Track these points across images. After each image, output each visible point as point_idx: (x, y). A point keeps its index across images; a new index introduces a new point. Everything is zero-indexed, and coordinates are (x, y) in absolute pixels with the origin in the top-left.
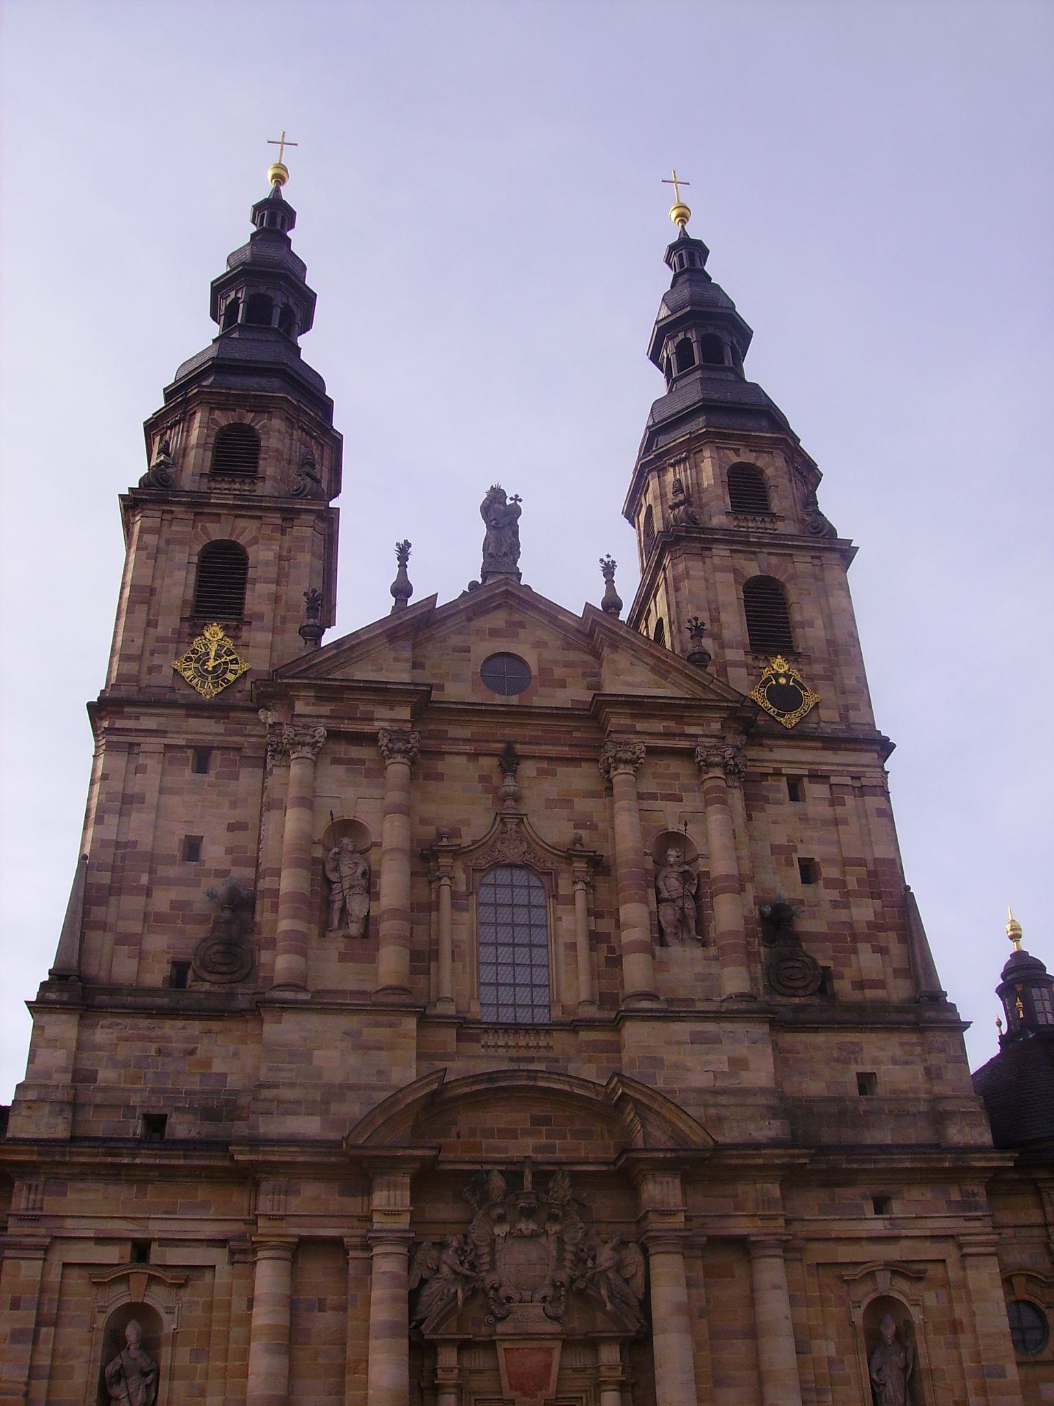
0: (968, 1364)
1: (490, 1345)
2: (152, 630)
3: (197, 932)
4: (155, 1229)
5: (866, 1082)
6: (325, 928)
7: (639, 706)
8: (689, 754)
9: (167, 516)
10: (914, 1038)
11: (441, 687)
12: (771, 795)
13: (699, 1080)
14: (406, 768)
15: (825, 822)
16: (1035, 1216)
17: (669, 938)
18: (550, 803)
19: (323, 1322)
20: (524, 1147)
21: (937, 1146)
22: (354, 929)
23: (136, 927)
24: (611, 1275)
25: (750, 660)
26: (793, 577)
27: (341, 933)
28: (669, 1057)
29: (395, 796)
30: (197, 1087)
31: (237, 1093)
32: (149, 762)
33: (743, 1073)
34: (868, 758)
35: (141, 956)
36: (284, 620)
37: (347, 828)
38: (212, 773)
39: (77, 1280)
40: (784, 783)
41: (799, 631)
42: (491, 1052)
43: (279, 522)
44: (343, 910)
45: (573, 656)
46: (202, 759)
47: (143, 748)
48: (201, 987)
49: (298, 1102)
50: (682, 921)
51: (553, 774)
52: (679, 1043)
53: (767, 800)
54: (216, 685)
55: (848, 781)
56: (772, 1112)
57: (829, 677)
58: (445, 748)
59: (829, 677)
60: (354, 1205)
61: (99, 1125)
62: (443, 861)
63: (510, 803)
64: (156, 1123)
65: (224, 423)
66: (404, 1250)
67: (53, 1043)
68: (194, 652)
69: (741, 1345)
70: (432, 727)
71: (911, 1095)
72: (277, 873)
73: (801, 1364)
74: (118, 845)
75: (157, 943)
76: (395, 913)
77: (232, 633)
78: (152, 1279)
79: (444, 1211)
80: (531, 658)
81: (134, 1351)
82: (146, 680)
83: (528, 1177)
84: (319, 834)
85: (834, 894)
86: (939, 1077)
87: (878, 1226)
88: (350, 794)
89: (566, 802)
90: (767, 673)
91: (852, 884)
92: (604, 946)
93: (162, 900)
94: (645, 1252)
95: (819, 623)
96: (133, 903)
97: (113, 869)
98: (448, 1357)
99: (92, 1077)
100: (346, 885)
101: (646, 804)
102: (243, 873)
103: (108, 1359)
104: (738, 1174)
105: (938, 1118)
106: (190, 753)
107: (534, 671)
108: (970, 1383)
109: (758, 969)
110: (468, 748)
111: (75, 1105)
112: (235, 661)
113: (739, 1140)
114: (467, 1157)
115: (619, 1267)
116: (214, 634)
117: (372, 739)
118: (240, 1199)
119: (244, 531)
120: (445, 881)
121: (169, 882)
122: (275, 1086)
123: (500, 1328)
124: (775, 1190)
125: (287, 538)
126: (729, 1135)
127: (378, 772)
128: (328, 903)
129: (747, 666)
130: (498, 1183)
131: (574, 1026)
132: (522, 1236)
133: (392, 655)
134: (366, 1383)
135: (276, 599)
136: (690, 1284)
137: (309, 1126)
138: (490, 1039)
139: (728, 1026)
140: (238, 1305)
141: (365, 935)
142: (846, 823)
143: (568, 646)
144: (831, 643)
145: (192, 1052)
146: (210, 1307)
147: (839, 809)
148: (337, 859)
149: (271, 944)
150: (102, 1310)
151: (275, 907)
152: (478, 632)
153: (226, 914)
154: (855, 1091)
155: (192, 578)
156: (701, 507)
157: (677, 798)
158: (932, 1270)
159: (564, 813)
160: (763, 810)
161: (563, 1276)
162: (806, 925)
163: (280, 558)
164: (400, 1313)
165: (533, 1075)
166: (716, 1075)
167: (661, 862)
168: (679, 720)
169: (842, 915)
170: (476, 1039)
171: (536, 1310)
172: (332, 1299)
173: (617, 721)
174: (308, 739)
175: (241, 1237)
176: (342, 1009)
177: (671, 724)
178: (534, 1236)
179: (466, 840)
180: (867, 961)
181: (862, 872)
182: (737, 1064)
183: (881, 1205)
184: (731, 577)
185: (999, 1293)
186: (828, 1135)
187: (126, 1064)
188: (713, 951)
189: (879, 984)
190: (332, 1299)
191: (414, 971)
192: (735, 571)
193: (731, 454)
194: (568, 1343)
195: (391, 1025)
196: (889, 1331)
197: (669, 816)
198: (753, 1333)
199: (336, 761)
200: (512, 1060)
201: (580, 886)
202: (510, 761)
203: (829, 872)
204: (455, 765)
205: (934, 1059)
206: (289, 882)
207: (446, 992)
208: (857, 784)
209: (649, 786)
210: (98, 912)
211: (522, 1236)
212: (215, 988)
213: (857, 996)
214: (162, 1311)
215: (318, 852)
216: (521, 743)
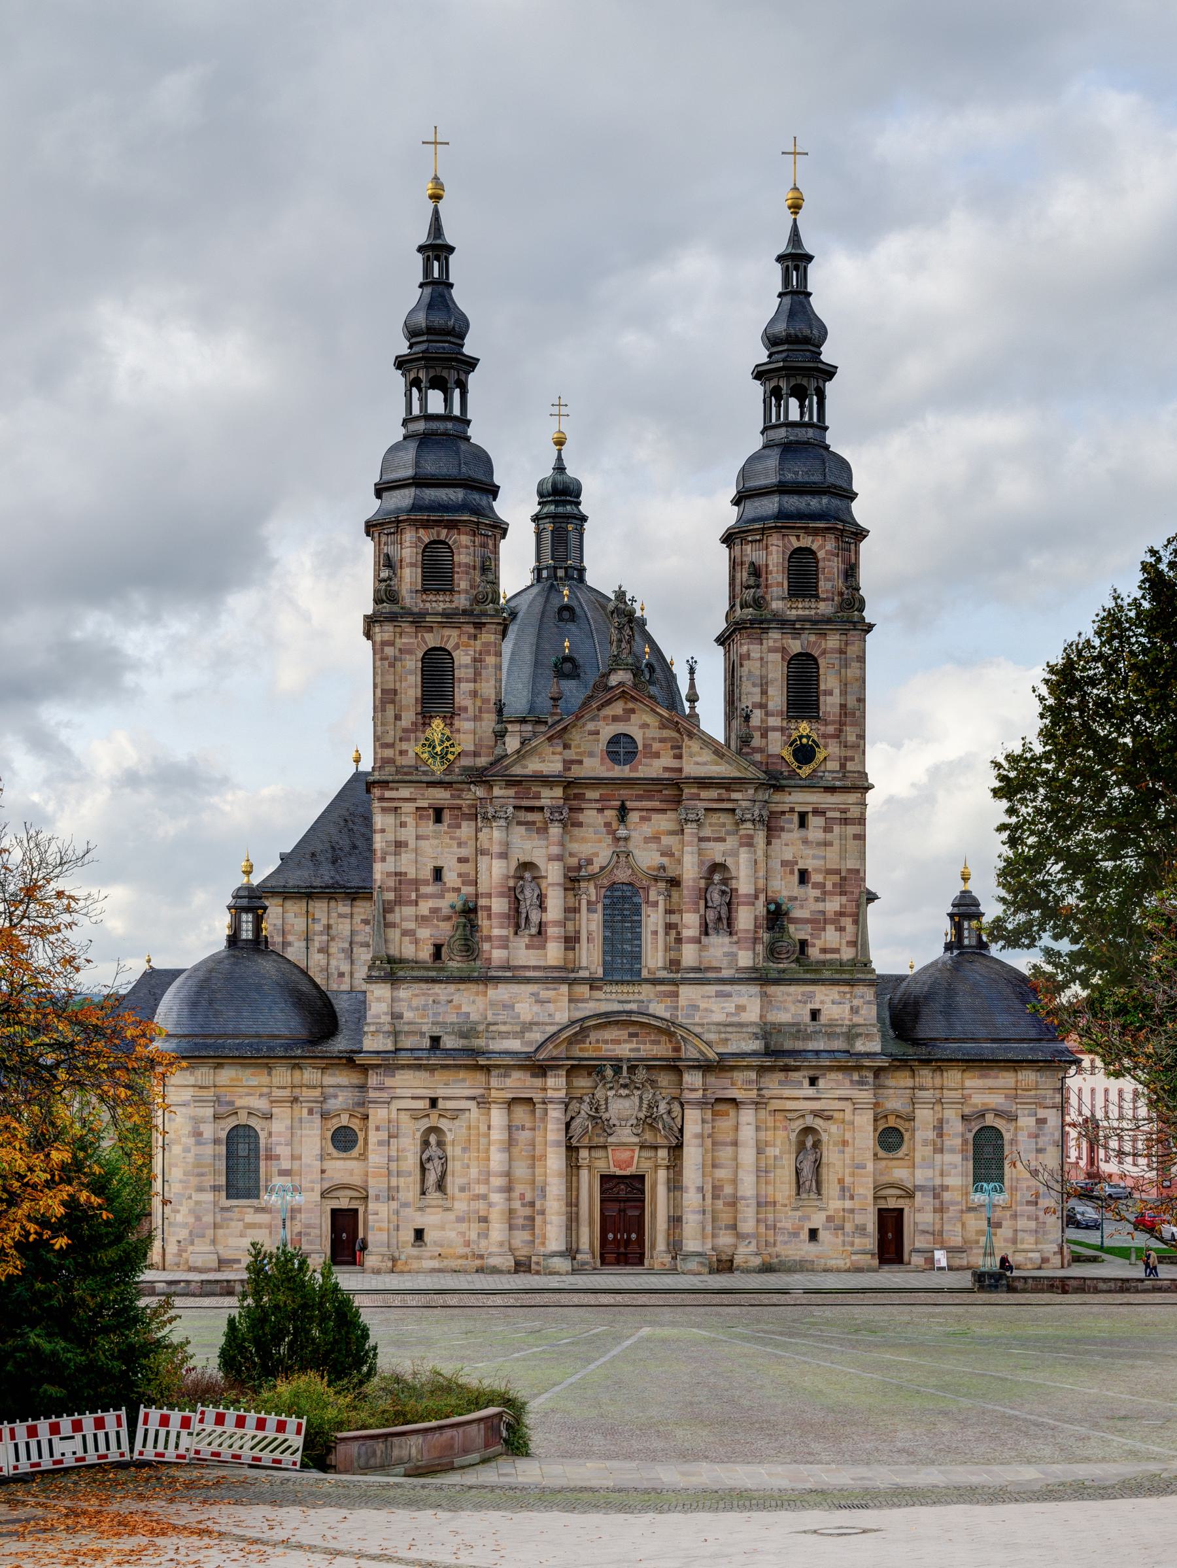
0: (848, 1162)
1: (605, 1147)
2: (398, 723)
3: (444, 931)
4: (440, 1093)
5: (815, 1014)
6: (517, 926)
7: (704, 783)
8: (733, 810)
9: (398, 630)
10: (847, 989)
11: (580, 762)
12: (786, 826)
13: (719, 1017)
14: (561, 830)
15: (819, 844)
16: (909, 1083)
17: (710, 931)
18: (647, 840)
19: (523, 1136)
20: (625, 1050)
21: (848, 1052)
22: (534, 931)
23: (411, 925)
24: (665, 1116)
25: (785, 724)
26: (824, 652)
27: (527, 932)
28: (703, 1005)
29: (555, 850)
30: (455, 1020)
31: (477, 1023)
32: (408, 819)
34: (852, 798)
35: (416, 942)
36: (480, 711)
37: (527, 866)
38: (446, 824)
39: (405, 1117)
40: (796, 818)
41: (822, 698)
42: (608, 996)
43: (472, 631)
44: (527, 917)
45: (667, 733)
46: (438, 815)
47: (403, 810)
48: (454, 963)
49: (508, 1033)
50: (720, 919)
51: (649, 819)
52: (709, 997)
53: (782, 829)
54: (442, 763)
55: (837, 815)
56: (756, 1036)
57: (837, 735)
58: (583, 806)
59: (838, 737)
60: (538, 1082)
61: (407, 1042)
62: (583, 884)
63: (622, 843)
64: (435, 1040)
65: (427, 540)
66: (563, 1106)
67: (379, 1000)
68: (427, 739)
69: (730, 1149)
70: (576, 791)
71: (840, 1022)
72: (489, 896)
73: (757, 1159)
74: (396, 874)
75: (424, 933)
76: (556, 923)
77: (448, 721)
78: (440, 1115)
79: (583, 1082)
80: (638, 736)
81: (434, 1148)
82: (402, 761)
83: (625, 1068)
84: (512, 873)
85: (817, 893)
86: (857, 1012)
87: (811, 1092)
88: (528, 845)
89: (656, 838)
90: (795, 734)
91: (829, 887)
92: (674, 932)
93: (424, 907)
94: (682, 1105)
95: (837, 692)
96: (409, 911)
97: (395, 890)
98: (584, 1153)
99: (400, 1016)
100: (528, 903)
101: (704, 845)
102: (468, 890)
103: (423, 1152)
104: (733, 1068)
106: (431, 811)
107: (640, 748)
108: (847, 1171)
109: (760, 948)
110: (598, 805)
111: (396, 1034)
112: (452, 745)
113: (737, 1051)
114: (594, 1055)
115: (669, 1112)
116: (437, 724)
117: (541, 809)
118: (480, 1077)
119: (450, 638)
120: (584, 896)
121: (427, 896)
122: (495, 1024)
123: (610, 1140)
124: (753, 1075)
125: (478, 642)
126: (732, 1048)
127: (543, 830)
128: (517, 911)
129: (782, 729)
130: (609, 1073)
131: (655, 982)
132: (621, 1096)
133: (551, 749)
134: (545, 1166)
135: (475, 694)
136: (703, 1121)
137: (515, 1045)
138: (607, 988)
139: (737, 988)
140: (483, 1128)
141: (540, 933)
142: (831, 844)
143: (663, 727)
144: (843, 706)
145: (451, 1001)
146: (469, 1128)
147: (829, 836)
148: (522, 887)
149: (489, 938)
150: (418, 1130)
151: (489, 917)
152: (605, 718)
153: (463, 920)
154: (807, 1018)
155: (419, 679)
156: (767, 586)
158: (836, 1115)
159: (654, 846)
160: (779, 837)
161: (642, 1115)
162: (797, 913)
163: (475, 660)
164: (561, 1136)
165: (630, 1012)
167: (709, 879)
168: (728, 789)
169: (820, 906)
170: (599, 989)
171: (628, 1131)
172: (528, 1125)
173: (687, 791)
174: (502, 814)
175: (483, 1096)
176: (528, 981)
177: (723, 791)
178: (627, 1096)
179: (595, 868)
180: (831, 936)
181: (836, 878)
182: (741, 1008)
183: (813, 1081)
184: (780, 655)
185: (871, 1128)
186: (788, 1045)
187: (417, 1009)
188: (735, 938)
189: (837, 951)
190: (528, 1125)
191: (566, 949)
192: (784, 650)
193: (793, 539)
194: (642, 1147)
195: (555, 989)
196: (809, 1144)
197: (716, 851)
198: (735, 1144)
199: (519, 823)
200: (619, 1002)
201: (661, 897)
203: (816, 878)
204: (590, 816)
205: (856, 1002)
206: (499, 905)
207: (584, 964)
208: (844, 816)
209: (707, 832)
210: (390, 917)
211: (621, 1096)
212: (459, 965)
213: (822, 957)
214: (445, 1129)
215: (511, 883)
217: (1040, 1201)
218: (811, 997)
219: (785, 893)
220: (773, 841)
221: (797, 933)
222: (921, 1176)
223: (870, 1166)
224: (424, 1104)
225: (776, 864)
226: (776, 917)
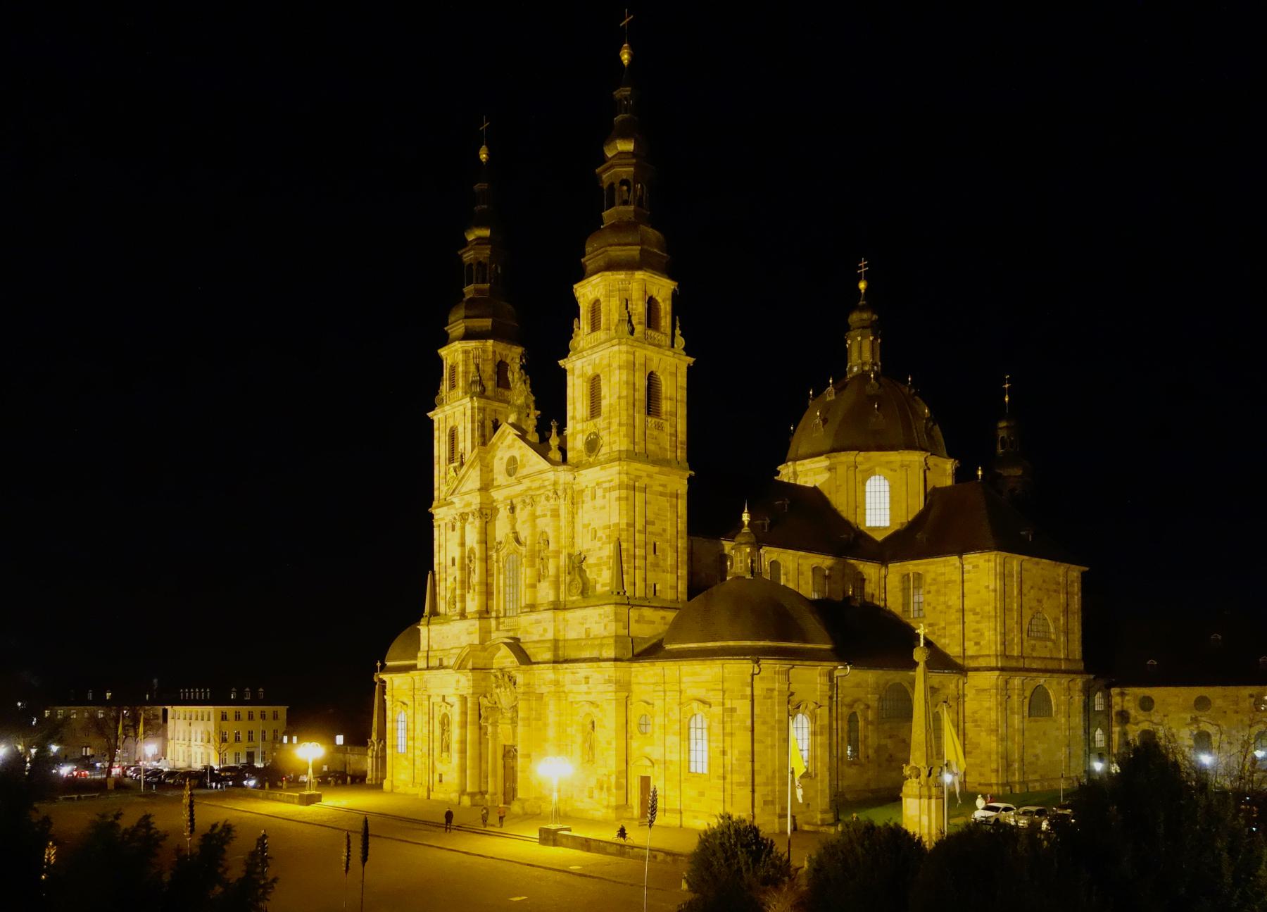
13: (536, 638)
33: (546, 635)
52: (532, 624)
53: (583, 502)
55: (606, 485)
87: (584, 688)
91: (604, 539)
95: (607, 397)
99: (432, 647)
105: (602, 646)
157: (545, 515)
162: (590, 561)
166: (541, 636)
182: (545, 630)
199: (469, 524)
202: (513, 509)
203: (599, 533)
204: (503, 513)
207: (495, 608)
216: (515, 497)
217: (729, 777)
218: (585, 619)
219: (585, 548)
220: (580, 511)
221: (590, 574)
222: (656, 753)
223: (614, 743)
224: (440, 699)
225: (579, 527)
226: (577, 565)
